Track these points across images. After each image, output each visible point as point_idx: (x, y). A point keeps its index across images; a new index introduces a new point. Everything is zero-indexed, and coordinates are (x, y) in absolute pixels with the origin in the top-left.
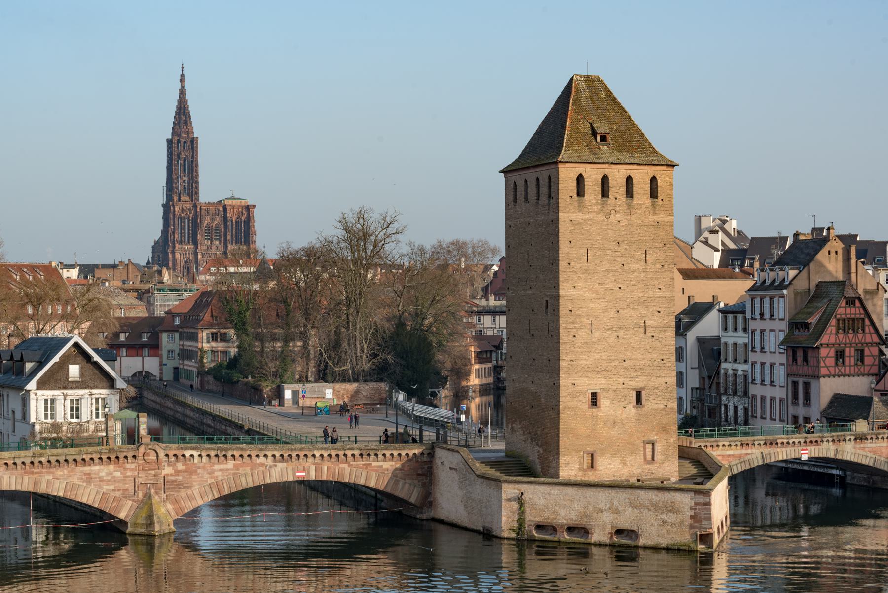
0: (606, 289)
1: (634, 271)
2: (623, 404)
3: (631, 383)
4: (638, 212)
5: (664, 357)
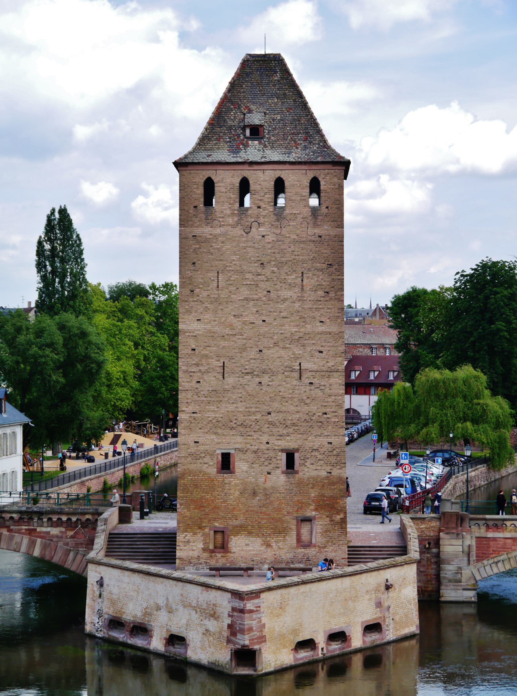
0: (244, 323)
1: (285, 300)
2: (267, 469)
3: (279, 443)
4: (292, 223)
5: (328, 410)
